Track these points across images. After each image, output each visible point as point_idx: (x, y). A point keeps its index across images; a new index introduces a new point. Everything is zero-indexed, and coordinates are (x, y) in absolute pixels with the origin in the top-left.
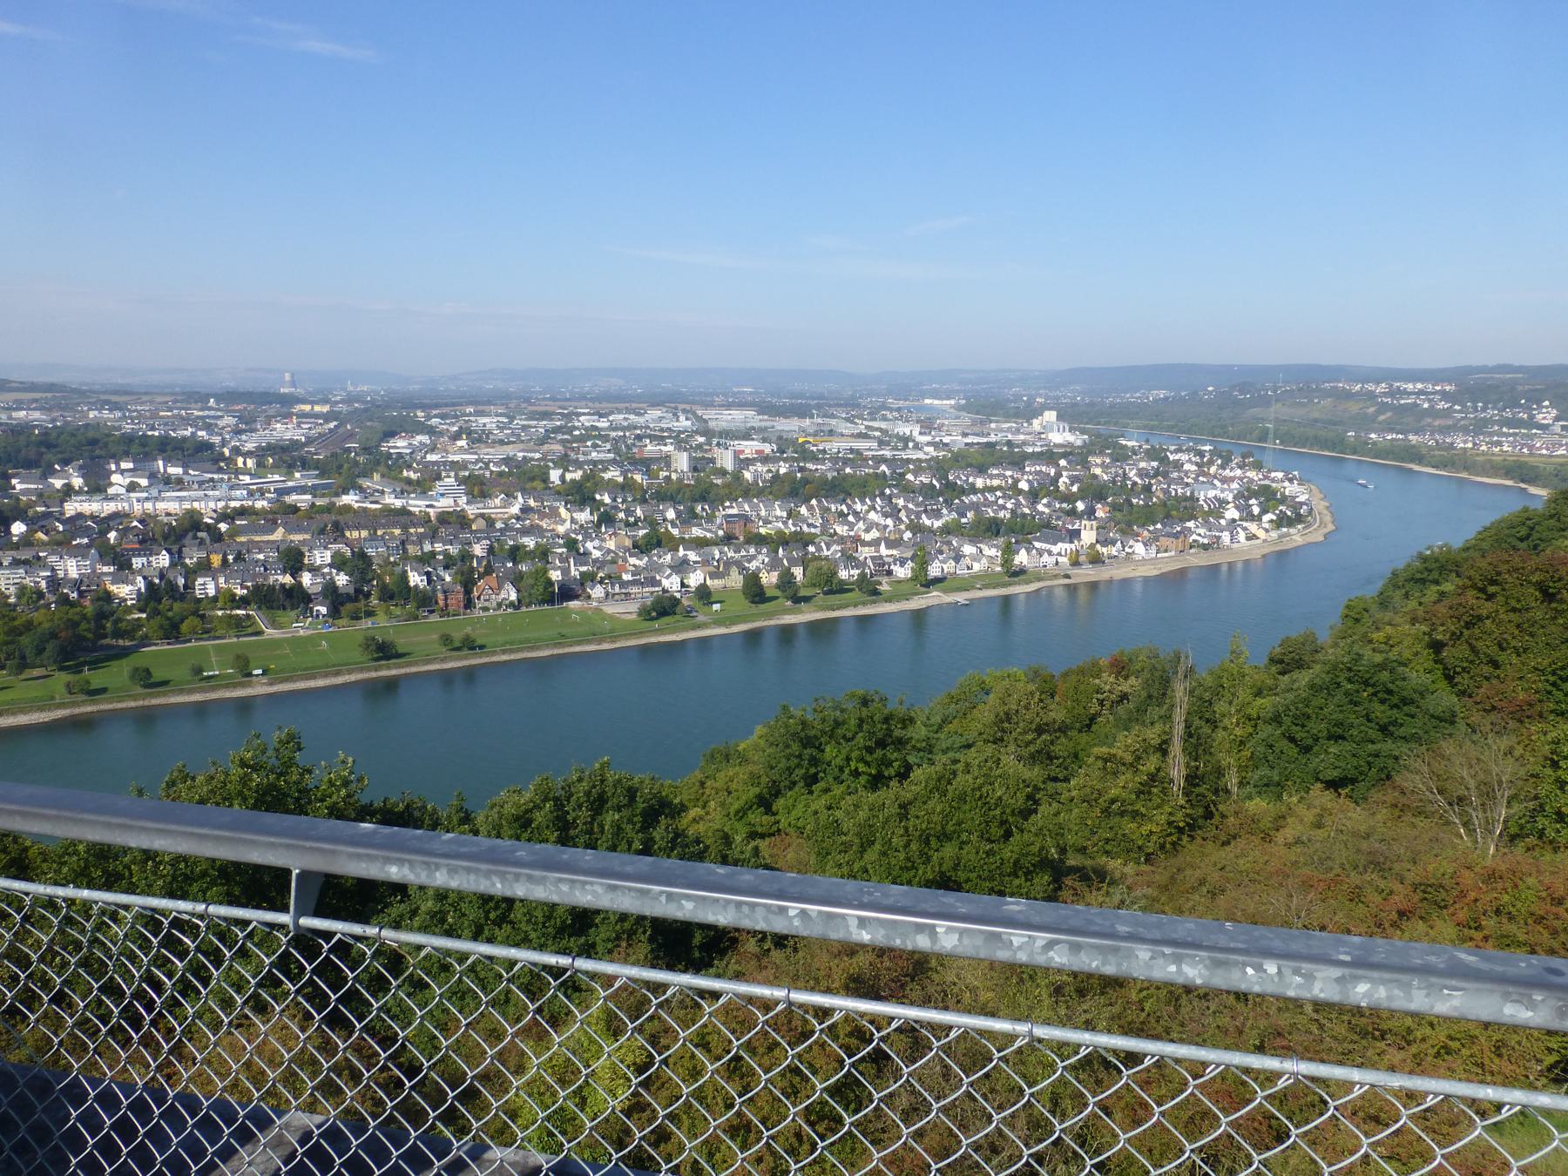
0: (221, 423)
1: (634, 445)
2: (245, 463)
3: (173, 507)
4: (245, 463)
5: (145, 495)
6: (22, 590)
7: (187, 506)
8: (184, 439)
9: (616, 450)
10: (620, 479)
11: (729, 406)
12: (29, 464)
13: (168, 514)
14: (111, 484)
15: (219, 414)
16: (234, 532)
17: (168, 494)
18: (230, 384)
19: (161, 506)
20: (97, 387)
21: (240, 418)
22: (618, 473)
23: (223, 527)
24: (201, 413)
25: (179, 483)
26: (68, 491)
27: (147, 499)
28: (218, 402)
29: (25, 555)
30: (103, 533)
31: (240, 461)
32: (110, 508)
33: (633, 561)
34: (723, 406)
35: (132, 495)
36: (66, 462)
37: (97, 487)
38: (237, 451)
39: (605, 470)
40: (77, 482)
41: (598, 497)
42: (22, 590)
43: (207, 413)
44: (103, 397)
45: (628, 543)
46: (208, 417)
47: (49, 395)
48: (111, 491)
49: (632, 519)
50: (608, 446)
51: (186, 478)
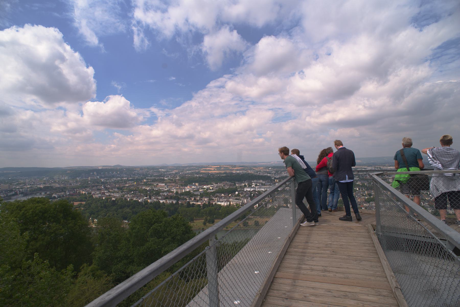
0: (272, 173)
1: (364, 176)
2: (277, 181)
4: (277, 181)
5: (259, 187)
6: (237, 204)
8: (265, 176)
9: (359, 177)
10: (361, 184)
11: (390, 166)
13: (262, 191)
14: (252, 185)
15: (272, 171)
18: (274, 165)
19: (261, 189)
20: (250, 166)
21: (276, 171)
22: (360, 183)
24: (268, 171)
26: (245, 186)
28: (272, 168)
29: (238, 198)
30: (251, 194)
31: (276, 180)
32: (252, 190)
33: (365, 204)
34: (388, 166)
35: (256, 187)
36: (245, 181)
37: (250, 186)
38: (275, 178)
39: (357, 182)
40: (247, 184)
41: (355, 189)
42: (237, 204)
43: (270, 171)
45: (364, 200)
46: (270, 171)
47: (242, 168)
48: (252, 186)
49: (364, 194)
50: (357, 176)
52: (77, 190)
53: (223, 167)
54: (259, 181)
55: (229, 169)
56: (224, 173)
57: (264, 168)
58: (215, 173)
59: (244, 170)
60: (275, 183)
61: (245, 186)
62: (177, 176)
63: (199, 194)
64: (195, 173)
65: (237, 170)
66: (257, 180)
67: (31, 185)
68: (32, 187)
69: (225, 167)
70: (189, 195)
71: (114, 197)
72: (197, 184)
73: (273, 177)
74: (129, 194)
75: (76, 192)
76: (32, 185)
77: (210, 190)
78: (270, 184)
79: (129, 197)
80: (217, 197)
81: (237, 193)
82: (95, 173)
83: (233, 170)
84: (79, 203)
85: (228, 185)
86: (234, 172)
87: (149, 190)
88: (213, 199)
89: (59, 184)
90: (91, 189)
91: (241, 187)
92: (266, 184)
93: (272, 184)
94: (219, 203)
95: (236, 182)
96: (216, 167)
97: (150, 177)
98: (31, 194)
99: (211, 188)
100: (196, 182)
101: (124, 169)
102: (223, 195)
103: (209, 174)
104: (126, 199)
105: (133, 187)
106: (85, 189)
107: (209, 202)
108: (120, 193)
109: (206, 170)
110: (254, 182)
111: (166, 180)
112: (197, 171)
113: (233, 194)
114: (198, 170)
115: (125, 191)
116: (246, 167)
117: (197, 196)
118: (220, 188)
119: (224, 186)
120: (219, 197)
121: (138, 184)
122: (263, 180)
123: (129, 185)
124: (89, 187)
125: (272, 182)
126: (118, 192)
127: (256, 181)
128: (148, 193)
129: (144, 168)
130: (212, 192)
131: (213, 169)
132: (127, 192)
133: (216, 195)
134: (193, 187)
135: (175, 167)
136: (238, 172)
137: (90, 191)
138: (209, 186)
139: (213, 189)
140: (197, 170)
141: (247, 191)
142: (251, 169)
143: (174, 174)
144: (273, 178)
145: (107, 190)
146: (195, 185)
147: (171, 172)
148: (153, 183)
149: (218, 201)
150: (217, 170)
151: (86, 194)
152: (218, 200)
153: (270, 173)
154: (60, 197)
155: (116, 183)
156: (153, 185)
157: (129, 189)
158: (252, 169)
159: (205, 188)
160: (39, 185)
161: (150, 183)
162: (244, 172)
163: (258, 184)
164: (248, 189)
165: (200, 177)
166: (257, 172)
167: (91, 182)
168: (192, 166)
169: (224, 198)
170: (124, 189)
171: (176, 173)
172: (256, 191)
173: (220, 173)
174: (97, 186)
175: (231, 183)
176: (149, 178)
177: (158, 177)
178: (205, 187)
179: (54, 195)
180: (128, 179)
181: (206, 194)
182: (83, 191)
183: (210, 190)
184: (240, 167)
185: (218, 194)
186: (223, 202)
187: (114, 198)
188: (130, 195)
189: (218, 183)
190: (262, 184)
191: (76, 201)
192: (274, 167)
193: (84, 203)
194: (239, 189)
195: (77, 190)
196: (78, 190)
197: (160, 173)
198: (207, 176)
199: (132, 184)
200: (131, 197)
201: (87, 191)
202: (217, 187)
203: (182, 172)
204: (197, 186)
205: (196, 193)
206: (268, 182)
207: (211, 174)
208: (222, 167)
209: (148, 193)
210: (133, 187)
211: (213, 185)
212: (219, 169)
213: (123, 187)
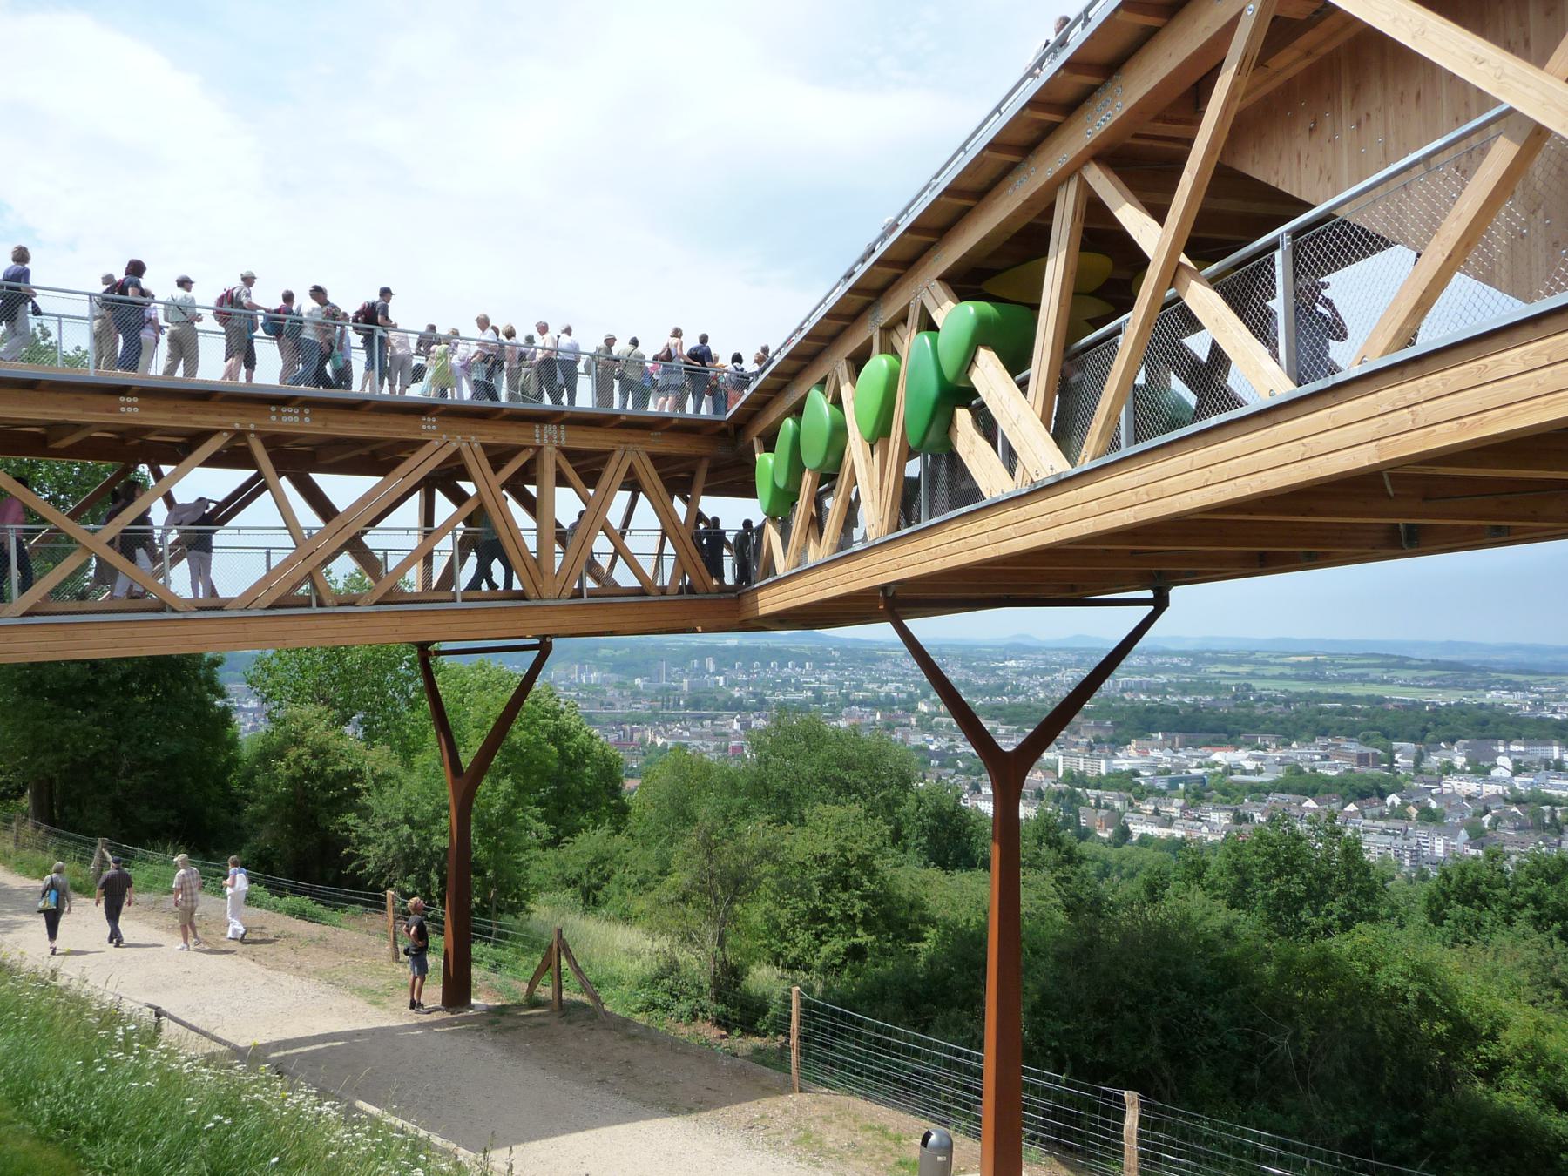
14: (1495, 766)
17: (1557, 782)
26: (1449, 769)
32: (1490, 789)
35: (1516, 778)
37: (1480, 770)
40: (1460, 761)
48: (1495, 773)
52: (633, 731)
66: (1533, 745)
70: (1129, 790)
75: (632, 737)
81: (1393, 799)
82: (710, 664)
87: (940, 755)
90: (688, 730)
106: (665, 727)
110: (1509, 754)
124: (680, 721)
127: (1522, 748)
135: (1072, 651)
137: (686, 738)
159: (1216, 764)
164: (1468, 786)
165: (1196, 708)
174: (713, 719)
182: (657, 733)
189: (1294, 745)
195: (633, 731)
196: (638, 730)
197: (998, 675)
201: (672, 737)
209: (935, 763)
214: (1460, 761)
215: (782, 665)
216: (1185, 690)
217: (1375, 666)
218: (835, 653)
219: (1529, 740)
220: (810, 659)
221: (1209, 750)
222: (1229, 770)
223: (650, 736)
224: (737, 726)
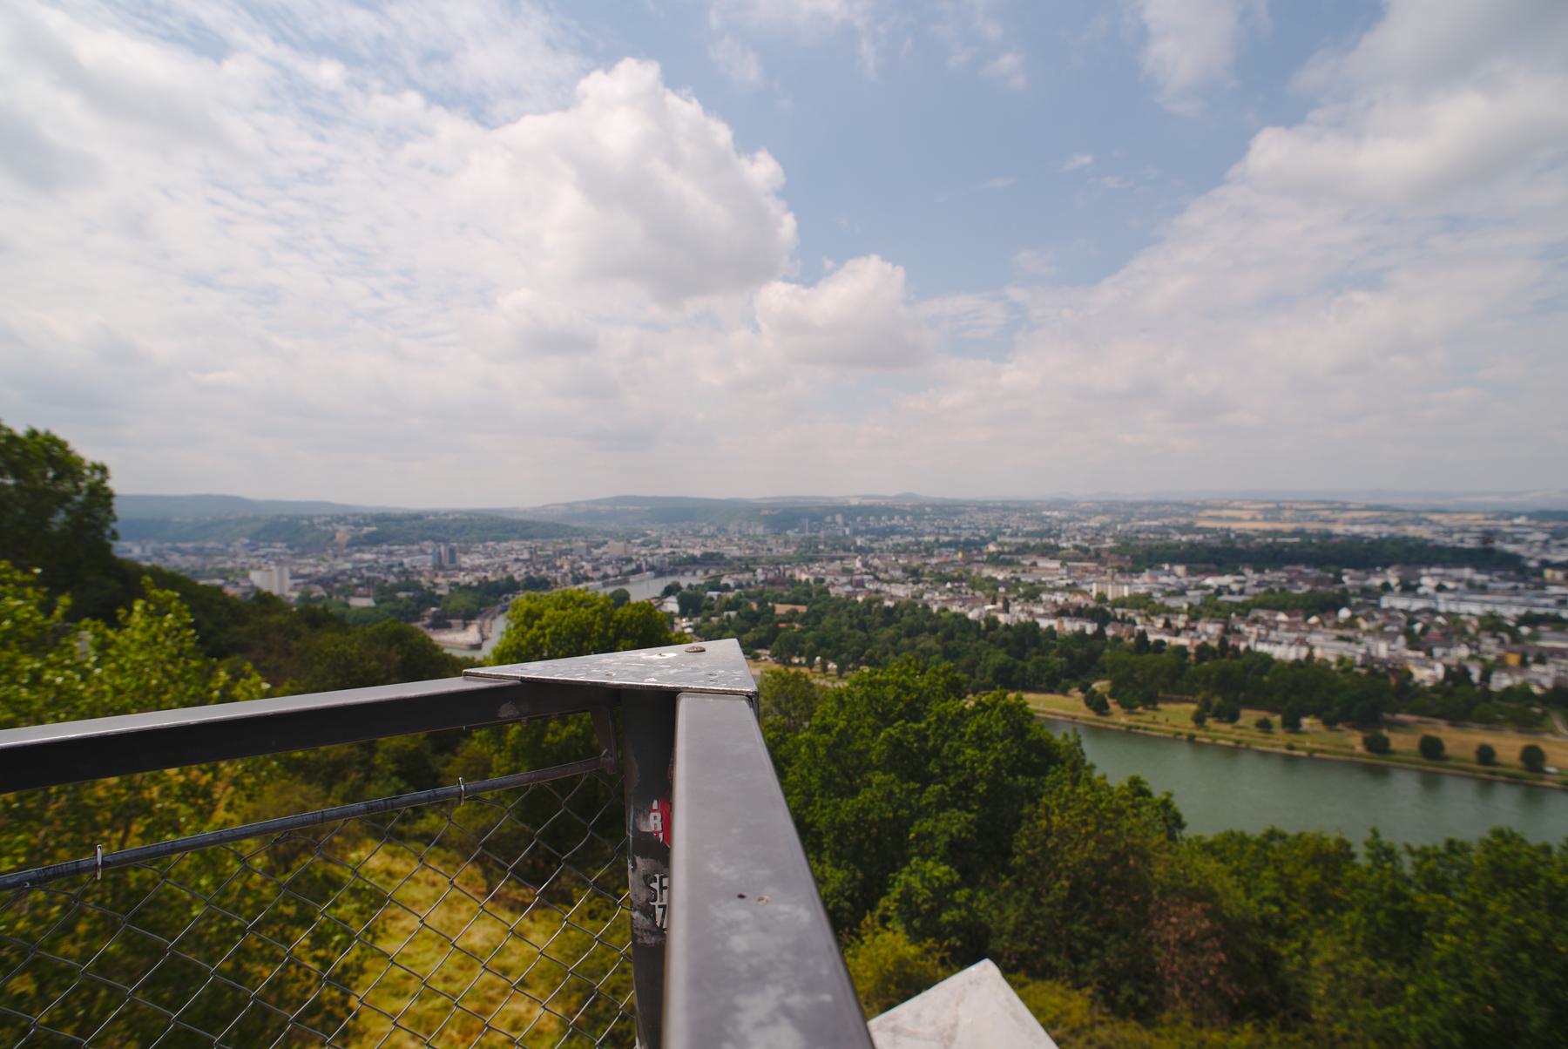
0: (1530, 538)
3: (1476, 609)
6: (1341, 660)
7: (1489, 608)
12: (1355, 567)
13: (1470, 614)
15: (1529, 530)
16: (1535, 637)
18: (1543, 504)
19: (1464, 608)
21: (1552, 534)
23: (1525, 630)
25: (1483, 589)
26: (1386, 587)
27: (1452, 600)
29: (1348, 633)
30: (1411, 622)
32: (1418, 605)
36: (1386, 566)
37: (1409, 588)
38: (1546, 564)
40: (1393, 581)
42: (1341, 660)
44: (1422, 515)
48: (1421, 591)
51: (1491, 585)
52: (785, 569)
53: (1291, 508)
54: (1456, 572)
55: (1316, 516)
56: (1294, 533)
57: (1487, 519)
58: (1256, 530)
59: (1385, 522)
60: (1542, 585)
61: (1386, 587)
62: (1104, 537)
63: (1185, 606)
64: (1174, 528)
65: (1354, 522)
67: (672, 547)
68: (673, 553)
69: (1297, 510)
70: (1145, 607)
71: (892, 597)
72: (1180, 569)
73: (1531, 559)
74: (936, 589)
76: (676, 547)
77: (1231, 593)
78: (1515, 588)
79: (935, 600)
80: (1255, 621)
81: (1344, 613)
82: (839, 518)
83: (1334, 521)
84: (789, 607)
85: (1306, 580)
86: (1338, 529)
87: (1005, 583)
88: (1239, 632)
89: (740, 549)
91: (1366, 592)
92: (1491, 585)
93: (1527, 588)
94: (1262, 648)
95: (1345, 571)
96: (1262, 506)
97: (1012, 535)
98: (673, 573)
99: (1235, 587)
100: (1175, 560)
101: (928, 506)
102: (1282, 617)
103: (1228, 535)
104: (926, 607)
105: (952, 569)
107: (1223, 642)
108: (911, 585)
109: (1219, 518)
110: (1432, 575)
111: (1064, 549)
112: (1183, 521)
113: (1329, 618)
114: (1187, 515)
115: (927, 581)
116: (1397, 510)
117: (1178, 613)
118: (1271, 591)
119: (1290, 581)
120: (1264, 623)
121: (969, 561)
122: (1478, 568)
123: (941, 560)
124: (817, 561)
125: (1525, 580)
126: (903, 583)
128: (1002, 590)
129: (990, 505)
130: (1238, 605)
131: (1248, 517)
132: (931, 583)
133: (1253, 614)
134: (1164, 579)
136: (1357, 529)
138: (1227, 580)
139: (1241, 592)
140: (1181, 515)
141: (1392, 609)
142: (1418, 522)
143: (1096, 528)
144: (1533, 564)
145: (871, 574)
146: (1170, 573)
147: (1084, 521)
148: (1020, 557)
149: (1260, 639)
150: (1265, 519)
151: (811, 581)
152: (1259, 635)
153: (1516, 541)
154: (739, 586)
155: (899, 552)
156: (1019, 564)
157: (940, 573)
158: (1425, 519)
159: (1208, 587)
160: (690, 547)
161: (1008, 557)
162: (1386, 530)
163: (1450, 585)
164: (1401, 603)
165: (1192, 544)
166: (1450, 533)
167: (826, 544)
168: (1166, 503)
169: (1288, 631)
170: (923, 574)
171: (1103, 527)
172: (1439, 614)
173: (1277, 533)
174: (842, 559)
175: (1323, 574)
176: (1007, 540)
177: (1037, 536)
178: (1209, 581)
179: (725, 581)
180: (937, 540)
181: (1211, 607)
182: (802, 571)
183: (1231, 593)
184: (1368, 508)
185: (1263, 614)
186: (1279, 643)
187: (890, 600)
188: (941, 594)
189: (1267, 571)
190: (1472, 586)
191: (781, 603)
192: (1541, 515)
193: (802, 609)
194: (1354, 600)
195: (785, 569)
196: (788, 569)
198: (1222, 542)
199: (949, 559)
200: (943, 601)
201: (812, 574)
202: (1259, 585)
203: (1124, 522)
204: (1179, 577)
205: (1172, 603)
206: (1505, 579)
207: (1239, 536)
208: (1284, 508)
209: (1002, 590)
210: (952, 569)
211: (1242, 574)
212: (1274, 513)
213: (919, 567)
214: (1393, 581)
215: (891, 519)
216: (1183, 530)
217: (1323, 509)
218: (928, 509)
219: (1445, 565)
220: (910, 514)
221: (1203, 577)
222: (1219, 592)
223: (797, 572)
224: (858, 564)
